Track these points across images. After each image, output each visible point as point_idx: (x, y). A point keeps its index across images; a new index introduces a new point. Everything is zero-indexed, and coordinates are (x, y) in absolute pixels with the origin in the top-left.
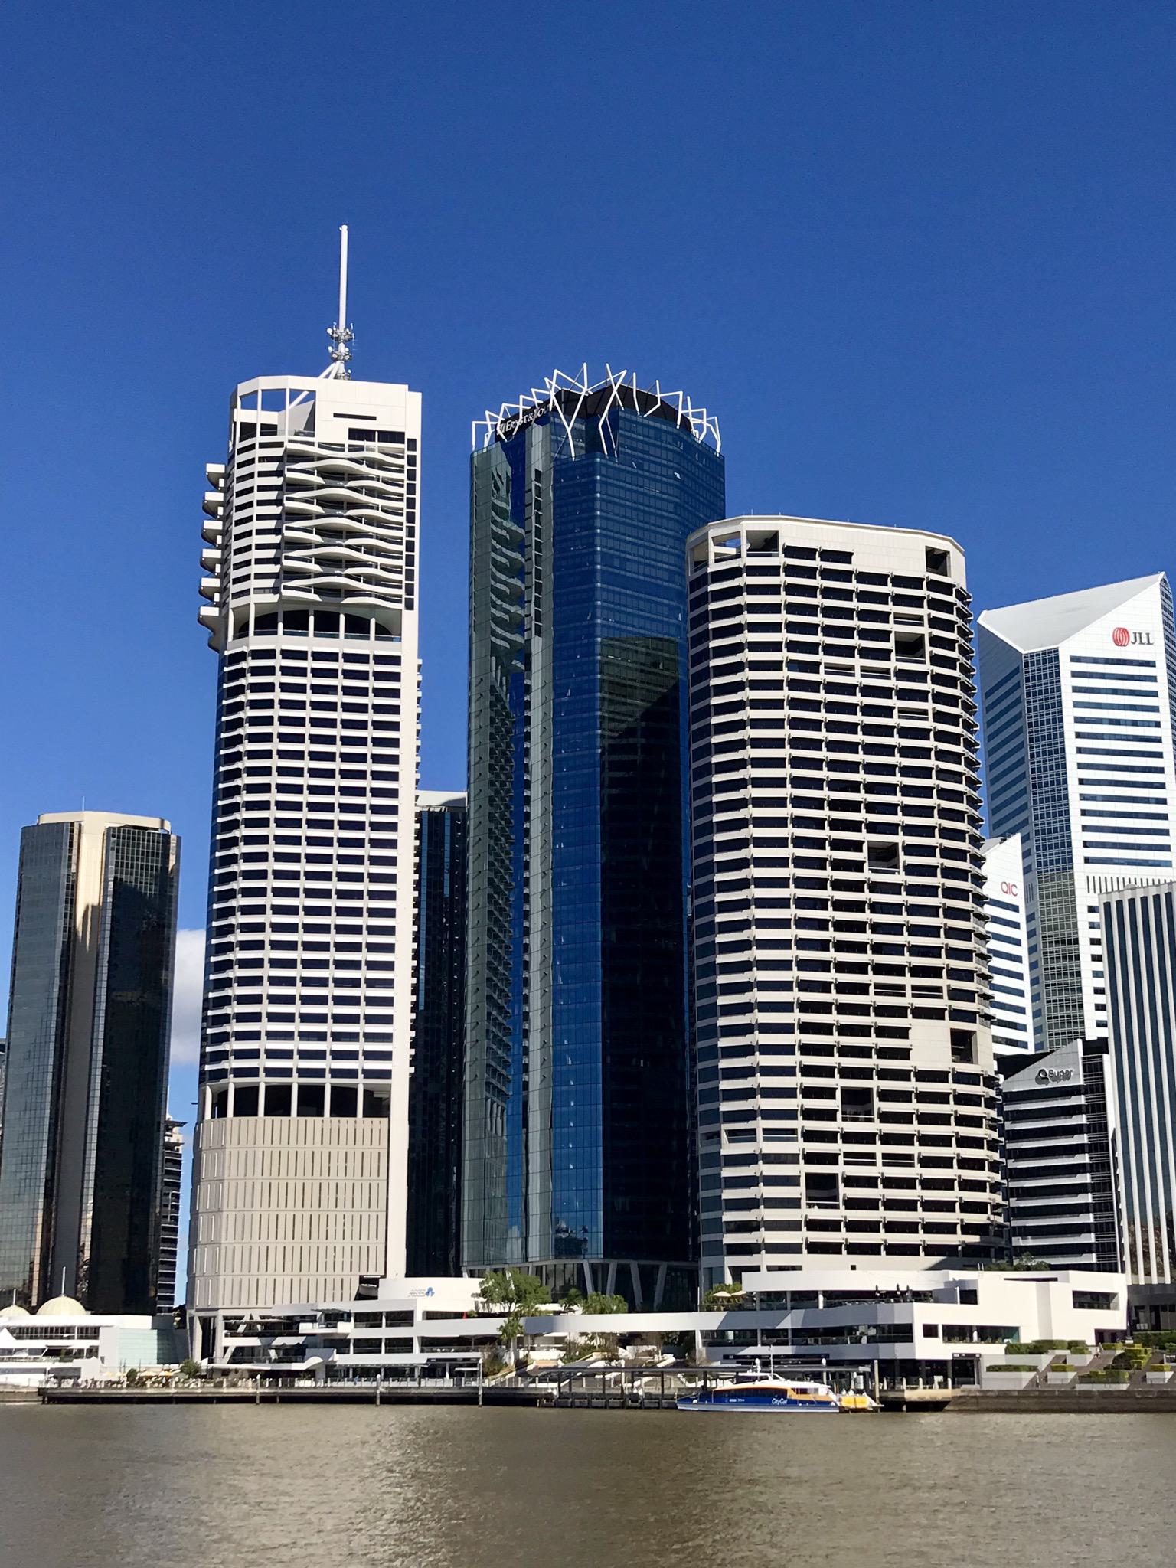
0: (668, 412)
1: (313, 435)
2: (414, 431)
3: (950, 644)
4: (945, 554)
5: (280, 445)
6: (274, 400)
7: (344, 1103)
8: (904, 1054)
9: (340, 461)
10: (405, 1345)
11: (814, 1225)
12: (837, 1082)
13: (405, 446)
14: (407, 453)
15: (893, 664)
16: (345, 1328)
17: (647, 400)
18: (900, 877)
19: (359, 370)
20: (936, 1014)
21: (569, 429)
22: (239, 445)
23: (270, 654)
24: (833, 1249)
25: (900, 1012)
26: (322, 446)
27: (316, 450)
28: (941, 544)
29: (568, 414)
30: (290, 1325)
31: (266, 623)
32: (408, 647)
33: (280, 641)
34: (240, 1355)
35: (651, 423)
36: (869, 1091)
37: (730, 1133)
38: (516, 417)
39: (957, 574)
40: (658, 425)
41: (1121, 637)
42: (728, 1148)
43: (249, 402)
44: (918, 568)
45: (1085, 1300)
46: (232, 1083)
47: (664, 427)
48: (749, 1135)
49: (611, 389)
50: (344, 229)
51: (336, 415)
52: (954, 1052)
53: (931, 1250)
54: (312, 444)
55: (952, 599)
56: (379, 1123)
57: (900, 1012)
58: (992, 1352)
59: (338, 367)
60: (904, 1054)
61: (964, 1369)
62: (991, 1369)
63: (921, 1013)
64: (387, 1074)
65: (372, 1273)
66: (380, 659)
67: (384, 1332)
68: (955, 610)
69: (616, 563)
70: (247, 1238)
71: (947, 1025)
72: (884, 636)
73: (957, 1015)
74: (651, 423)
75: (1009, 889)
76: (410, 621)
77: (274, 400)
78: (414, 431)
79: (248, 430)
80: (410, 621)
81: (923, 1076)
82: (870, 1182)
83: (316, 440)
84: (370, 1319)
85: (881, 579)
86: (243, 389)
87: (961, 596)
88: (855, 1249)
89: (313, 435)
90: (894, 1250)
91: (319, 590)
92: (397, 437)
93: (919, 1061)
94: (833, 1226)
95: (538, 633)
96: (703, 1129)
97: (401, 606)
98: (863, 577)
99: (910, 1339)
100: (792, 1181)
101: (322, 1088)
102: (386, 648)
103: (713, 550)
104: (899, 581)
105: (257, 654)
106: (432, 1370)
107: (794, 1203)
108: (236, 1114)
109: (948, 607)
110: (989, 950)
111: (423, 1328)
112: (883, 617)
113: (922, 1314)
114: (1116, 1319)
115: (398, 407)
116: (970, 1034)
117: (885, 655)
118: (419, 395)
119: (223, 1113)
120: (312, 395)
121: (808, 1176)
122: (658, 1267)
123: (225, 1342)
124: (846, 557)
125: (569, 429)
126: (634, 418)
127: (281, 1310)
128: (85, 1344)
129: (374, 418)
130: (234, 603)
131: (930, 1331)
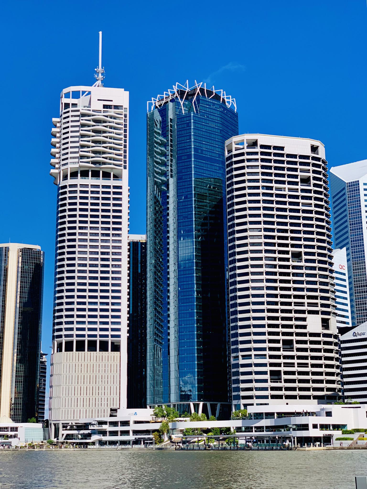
0: (217, 97)
1: (90, 107)
2: (126, 105)
3: (319, 179)
4: (317, 147)
5: (78, 111)
6: (76, 95)
7: (104, 347)
8: (305, 327)
10: (126, 433)
11: (273, 389)
12: (281, 337)
13: (123, 111)
14: (124, 113)
15: (299, 187)
16: (104, 427)
17: (210, 93)
18: (303, 264)
19: (106, 84)
20: (316, 312)
21: (182, 104)
22: (64, 111)
23: (75, 186)
24: (280, 397)
25: (303, 312)
26: (93, 111)
27: (91, 112)
28: (316, 143)
29: (182, 98)
30: (85, 426)
31: (74, 175)
32: (124, 182)
33: (79, 181)
34: (68, 437)
35: (212, 101)
36: (292, 341)
37: (243, 356)
38: (162, 100)
40: (214, 102)
42: (242, 361)
43: (67, 96)
44: (308, 152)
46: (64, 340)
47: (216, 102)
50: (100, 33)
51: (98, 100)
52: (323, 326)
53: (315, 397)
54: (90, 110)
55: (320, 163)
56: (116, 354)
57: (303, 312)
58: (337, 434)
59: (99, 82)
60: (305, 327)
61: (327, 440)
62: (337, 439)
63: (310, 312)
64: (119, 336)
65: (114, 407)
66: (115, 187)
67: (120, 428)
68: (322, 167)
69: (200, 151)
70: (70, 395)
71: (320, 316)
72: (296, 177)
73: (323, 313)
74: (212, 101)
77: (76, 95)
79: (67, 105)
80: (125, 173)
81: (311, 335)
82: (293, 373)
83: (91, 109)
84: (114, 424)
85: (295, 156)
86: (65, 91)
87: (323, 162)
88: (288, 397)
89: (90, 107)
90: (302, 397)
93: (310, 330)
94: (280, 389)
95: (172, 176)
96: (233, 355)
97: (122, 168)
98: (288, 156)
99: (308, 429)
100: (265, 373)
101: (96, 341)
103: (234, 146)
104: (301, 157)
107: (266, 381)
108: (65, 351)
109: (319, 166)
110: (335, 289)
111: (133, 427)
112: (296, 170)
113: (311, 421)
115: (121, 97)
116: (328, 319)
117: (296, 183)
118: (128, 93)
119: (61, 351)
120: (89, 93)
121: (270, 371)
122: (217, 404)
123: (63, 432)
124: (282, 148)
125: (182, 104)
126: (205, 99)
127: (82, 421)
128: (13, 433)
129: (112, 101)
130: (62, 168)
131: (315, 426)
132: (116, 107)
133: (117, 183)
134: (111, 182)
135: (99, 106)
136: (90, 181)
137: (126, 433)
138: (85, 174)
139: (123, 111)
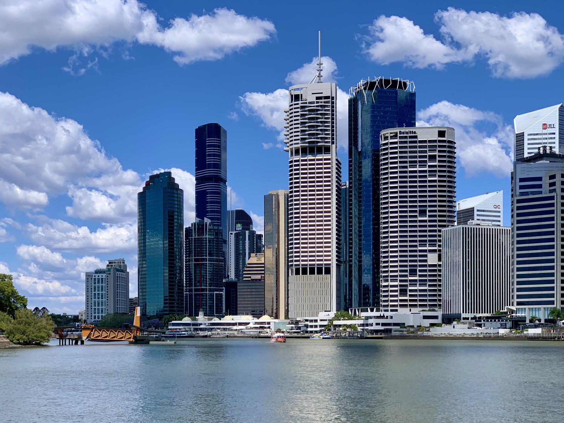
9: (313, 106)
10: (316, 326)
41: (545, 126)
44: (436, 137)
45: (425, 317)
48: (387, 281)
49: (375, 82)
57: (425, 251)
63: (430, 251)
75: (496, 207)
85: (425, 141)
91: (309, 142)
97: (330, 144)
98: (420, 142)
104: (430, 141)
105: (296, 161)
111: (319, 323)
128: (267, 326)
131: (377, 324)
135: (313, 98)
137: (316, 326)
139: (330, 100)
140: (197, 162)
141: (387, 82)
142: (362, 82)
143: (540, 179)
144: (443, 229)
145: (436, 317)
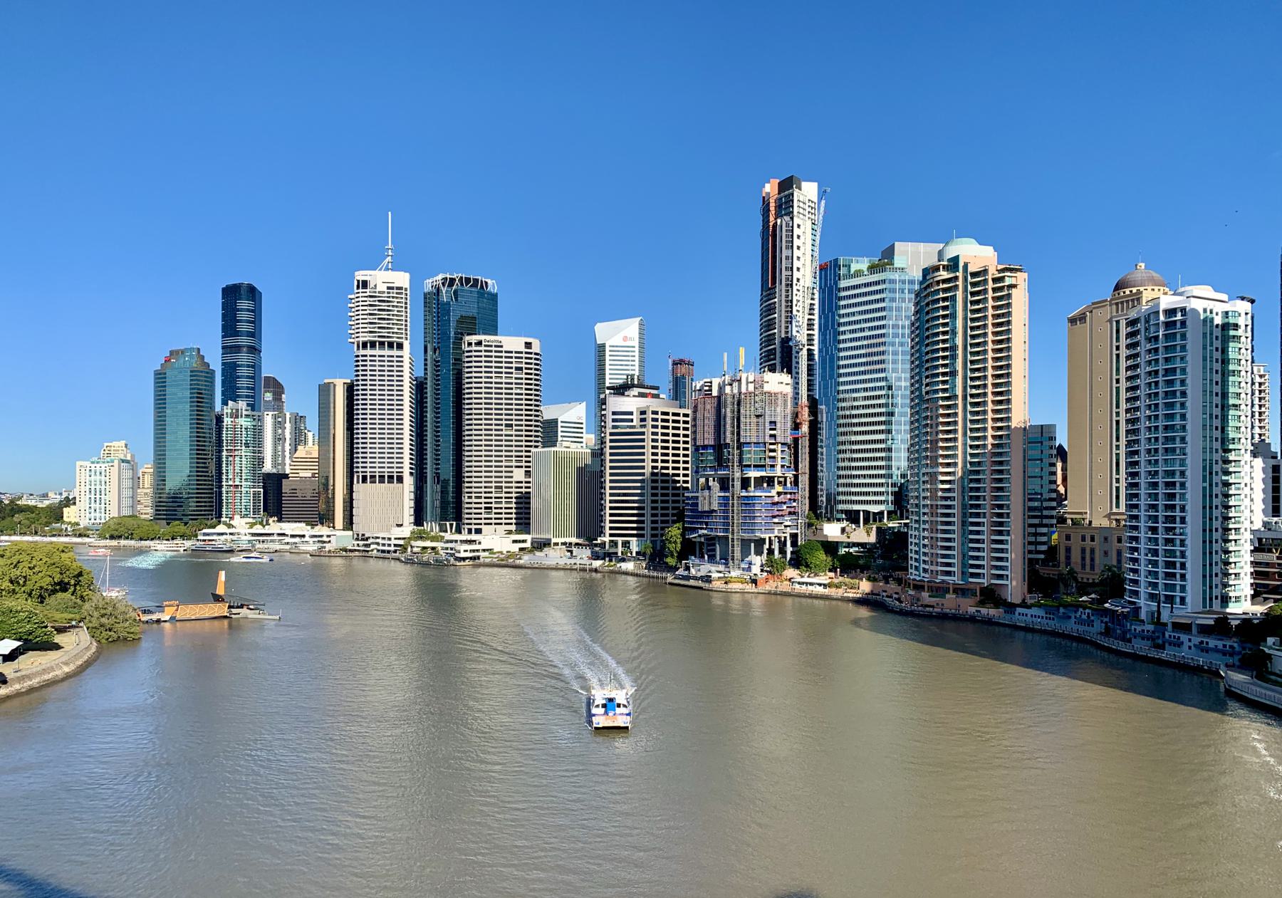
2: (406, 284)
9: (384, 296)
31: (365, 345)
33: (369, 352)
39: (536, 348)
45: (515, 541)
58: (486, 554)
67: (386, 542)
76: (406, 345)
78: (406, 284)
92: (400, 288)
102: (399, 353)
106: (395, 552)
111: (393, 542)
114: (528, 545)
115: (402, 279)
132: (398, 288)
133: (399, 353)
134: (395, 352)
136: (377, 352)
138: (373, 345)
140: (224, 328)
141: (468, 280)
142: (440, 277)
143: (631, 413)
144: (533, 450)
145: (524, 541)
